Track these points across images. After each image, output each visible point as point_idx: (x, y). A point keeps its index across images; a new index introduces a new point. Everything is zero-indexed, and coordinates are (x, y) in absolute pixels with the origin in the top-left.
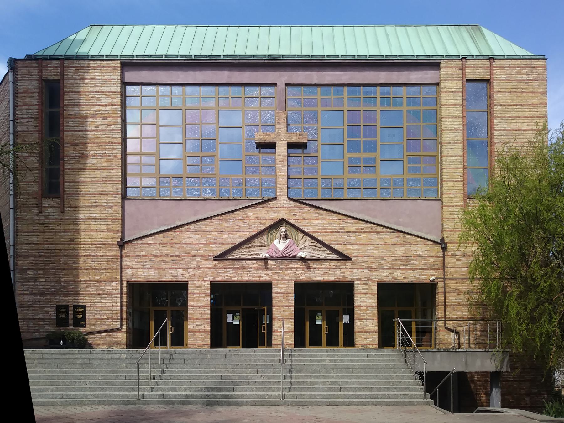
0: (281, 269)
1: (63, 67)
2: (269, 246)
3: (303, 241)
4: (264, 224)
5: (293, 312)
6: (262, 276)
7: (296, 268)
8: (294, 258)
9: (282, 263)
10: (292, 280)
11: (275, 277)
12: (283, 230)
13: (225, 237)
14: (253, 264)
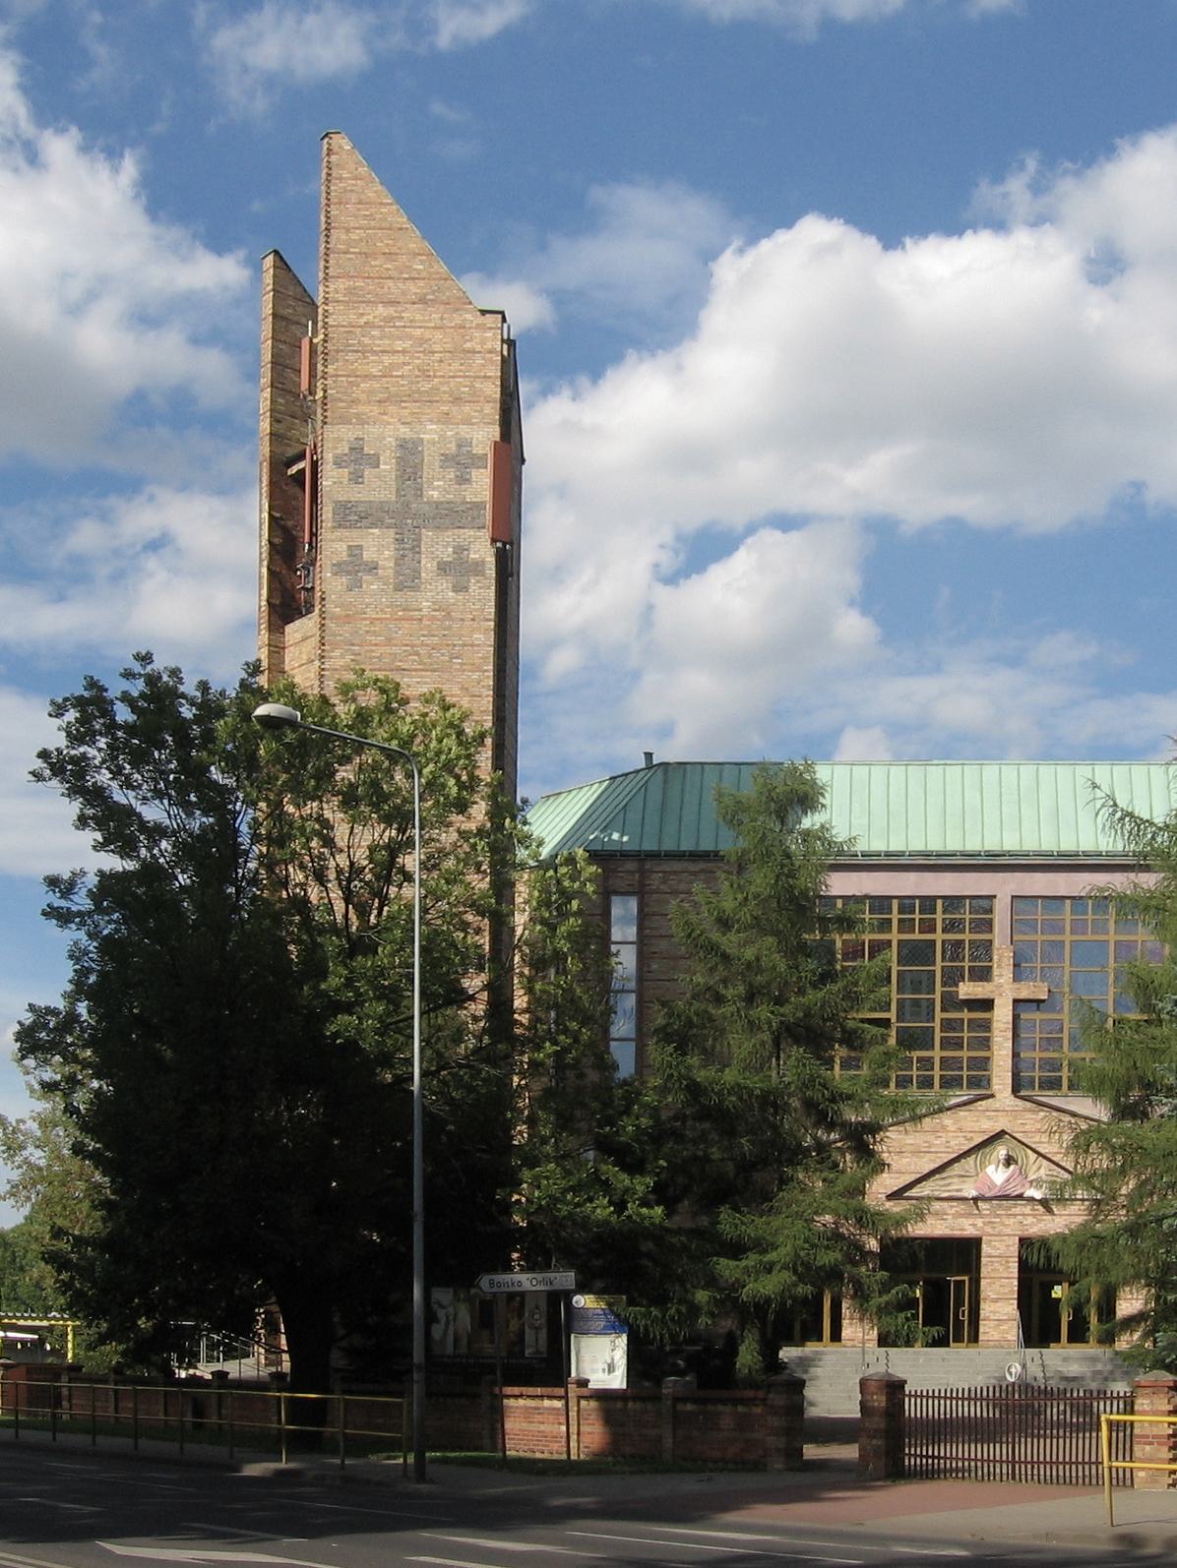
0: (999, 1216)
1: (642, 872)
2: (977, 1175)
3: (1035, 1168)
4: (972, 1139)
5: (1016, 1288)
6: (966, 1228)
7: (1023, 1215)
8: (1020, 1197)
9: (1000, 1206)
10: (1014, 1235)
11: (988, 1229)
12: (1001, 1152)
13: (904, 1160)
14: (952, 1207)
